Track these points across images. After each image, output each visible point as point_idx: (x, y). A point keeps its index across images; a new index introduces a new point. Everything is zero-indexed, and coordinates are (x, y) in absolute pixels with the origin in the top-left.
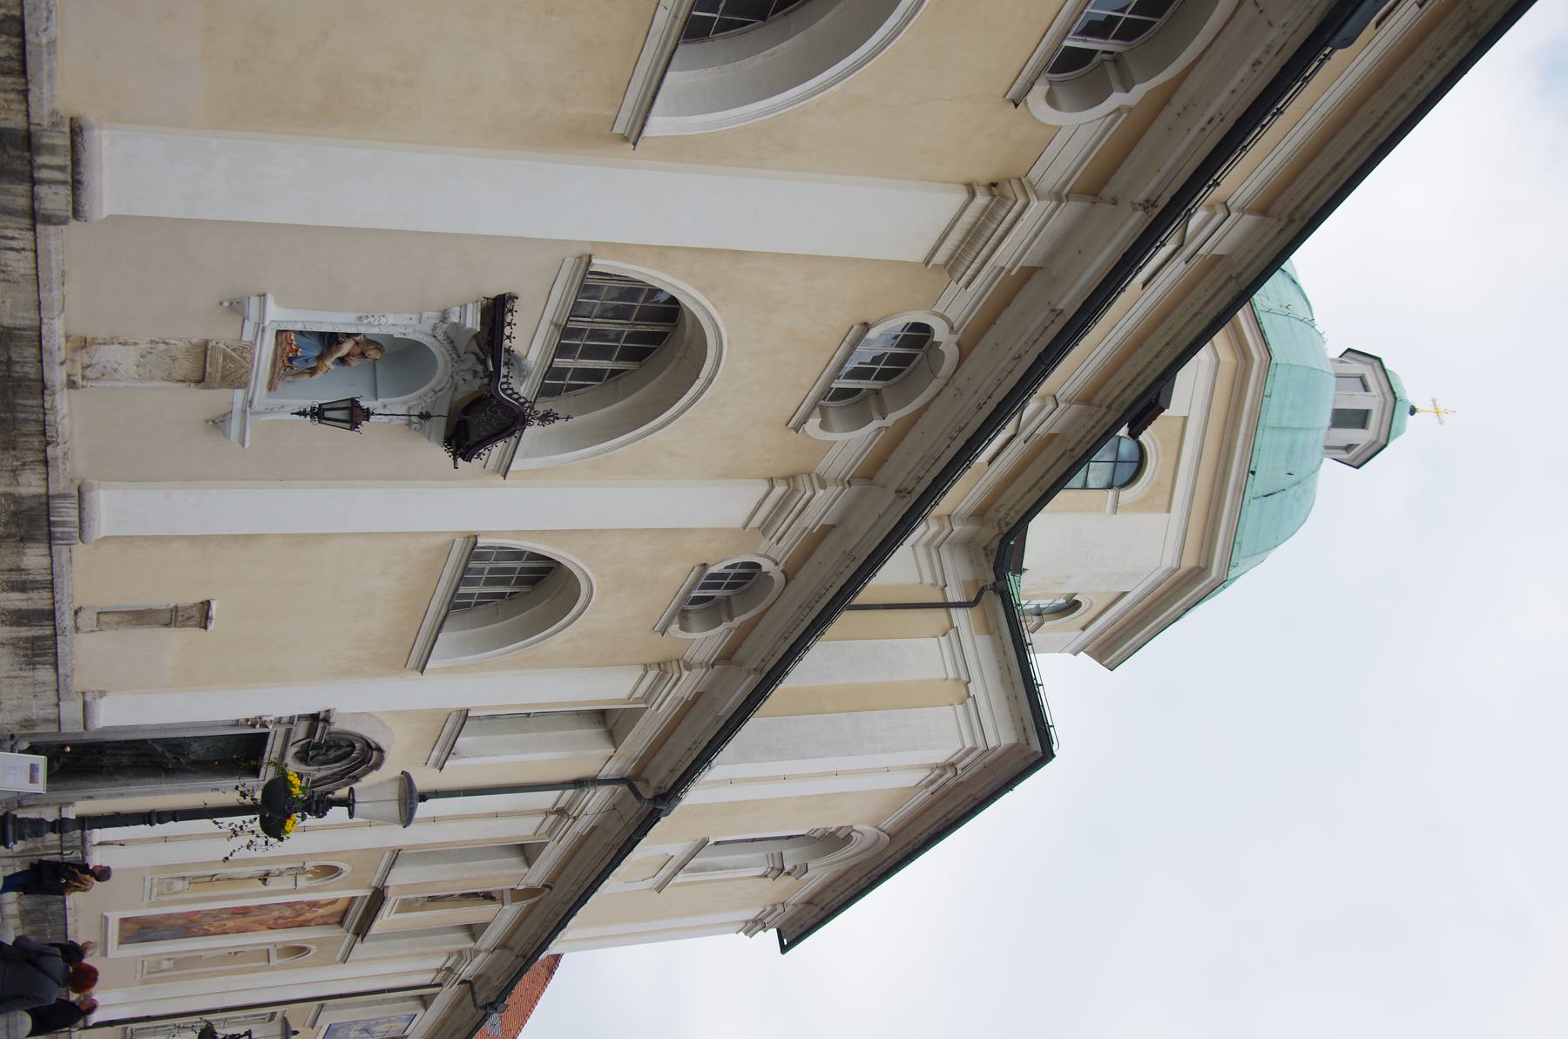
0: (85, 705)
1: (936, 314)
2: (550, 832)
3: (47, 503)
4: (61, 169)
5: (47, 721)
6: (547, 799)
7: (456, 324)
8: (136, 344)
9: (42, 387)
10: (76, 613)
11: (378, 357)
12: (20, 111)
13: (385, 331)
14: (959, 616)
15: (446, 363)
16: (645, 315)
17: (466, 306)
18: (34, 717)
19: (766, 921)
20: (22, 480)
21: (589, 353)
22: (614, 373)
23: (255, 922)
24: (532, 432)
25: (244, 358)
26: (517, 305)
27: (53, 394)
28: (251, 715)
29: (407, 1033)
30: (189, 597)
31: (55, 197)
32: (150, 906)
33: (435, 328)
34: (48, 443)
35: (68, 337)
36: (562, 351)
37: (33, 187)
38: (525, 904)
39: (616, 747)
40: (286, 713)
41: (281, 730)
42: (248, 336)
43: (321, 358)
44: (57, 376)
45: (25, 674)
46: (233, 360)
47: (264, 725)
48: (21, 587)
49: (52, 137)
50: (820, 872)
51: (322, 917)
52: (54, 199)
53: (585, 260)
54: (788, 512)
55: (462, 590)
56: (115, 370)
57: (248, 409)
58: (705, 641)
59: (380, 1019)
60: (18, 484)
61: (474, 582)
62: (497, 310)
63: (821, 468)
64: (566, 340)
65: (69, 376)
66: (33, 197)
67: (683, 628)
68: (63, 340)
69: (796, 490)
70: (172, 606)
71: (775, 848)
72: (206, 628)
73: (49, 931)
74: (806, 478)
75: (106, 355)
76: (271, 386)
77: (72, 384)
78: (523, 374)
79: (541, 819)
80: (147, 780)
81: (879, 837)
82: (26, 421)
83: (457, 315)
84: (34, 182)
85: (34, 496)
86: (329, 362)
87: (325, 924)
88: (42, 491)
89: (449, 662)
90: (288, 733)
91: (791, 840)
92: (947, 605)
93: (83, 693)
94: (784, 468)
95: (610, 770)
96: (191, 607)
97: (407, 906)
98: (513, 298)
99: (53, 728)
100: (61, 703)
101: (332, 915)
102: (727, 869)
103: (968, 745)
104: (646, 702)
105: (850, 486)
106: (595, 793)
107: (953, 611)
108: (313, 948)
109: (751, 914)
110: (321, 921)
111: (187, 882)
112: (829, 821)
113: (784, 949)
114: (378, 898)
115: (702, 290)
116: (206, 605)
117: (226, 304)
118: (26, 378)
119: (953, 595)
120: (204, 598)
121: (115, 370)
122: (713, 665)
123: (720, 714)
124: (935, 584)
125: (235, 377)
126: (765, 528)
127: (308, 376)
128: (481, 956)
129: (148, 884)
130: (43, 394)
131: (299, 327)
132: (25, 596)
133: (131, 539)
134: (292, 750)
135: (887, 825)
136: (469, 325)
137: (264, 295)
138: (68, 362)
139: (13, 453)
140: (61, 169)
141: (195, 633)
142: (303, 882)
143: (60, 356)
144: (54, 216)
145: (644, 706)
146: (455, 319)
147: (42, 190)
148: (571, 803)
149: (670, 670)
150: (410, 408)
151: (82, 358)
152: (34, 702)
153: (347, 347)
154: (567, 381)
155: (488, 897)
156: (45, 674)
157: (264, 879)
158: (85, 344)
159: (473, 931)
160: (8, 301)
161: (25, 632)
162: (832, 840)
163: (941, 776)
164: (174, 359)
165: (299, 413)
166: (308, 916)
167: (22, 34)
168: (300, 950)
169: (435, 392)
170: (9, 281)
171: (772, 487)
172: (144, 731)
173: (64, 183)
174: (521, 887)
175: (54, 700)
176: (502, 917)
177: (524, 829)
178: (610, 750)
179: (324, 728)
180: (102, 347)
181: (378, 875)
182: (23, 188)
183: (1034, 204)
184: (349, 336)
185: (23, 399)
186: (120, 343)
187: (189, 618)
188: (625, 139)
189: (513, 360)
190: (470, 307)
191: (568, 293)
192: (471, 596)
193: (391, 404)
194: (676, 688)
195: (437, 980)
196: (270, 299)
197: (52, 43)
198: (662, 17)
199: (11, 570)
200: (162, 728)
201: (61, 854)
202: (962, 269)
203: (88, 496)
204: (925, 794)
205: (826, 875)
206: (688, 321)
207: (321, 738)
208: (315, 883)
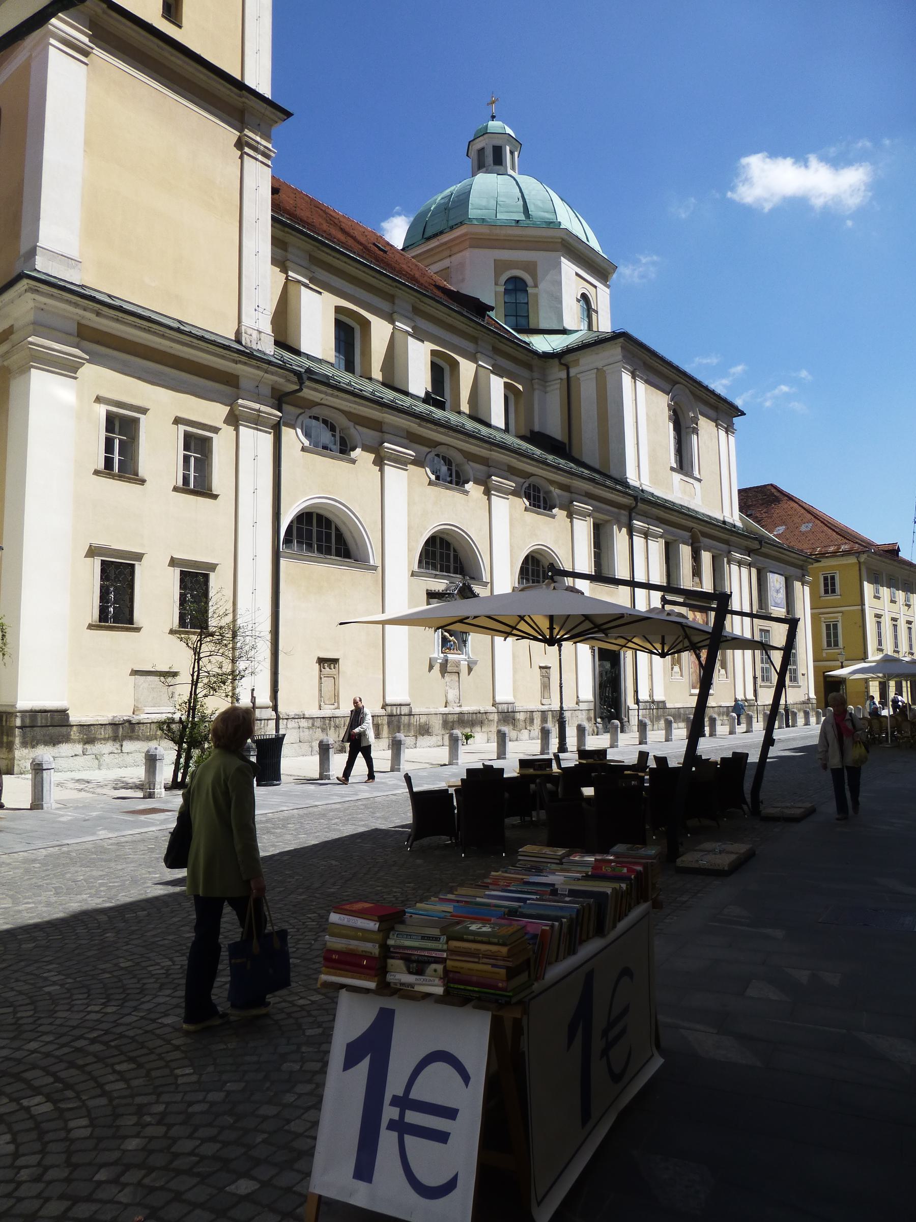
4: (397, 708)
5: (588, 713)
14: (573, 372)
44: (458, 710)
48: (532, 721)
52: (405, 710)
98: (427, 590)
99: (592, 712)
119: (563, 375)
140: (397, 708)
164: (452, 680)
201: (653, 709)
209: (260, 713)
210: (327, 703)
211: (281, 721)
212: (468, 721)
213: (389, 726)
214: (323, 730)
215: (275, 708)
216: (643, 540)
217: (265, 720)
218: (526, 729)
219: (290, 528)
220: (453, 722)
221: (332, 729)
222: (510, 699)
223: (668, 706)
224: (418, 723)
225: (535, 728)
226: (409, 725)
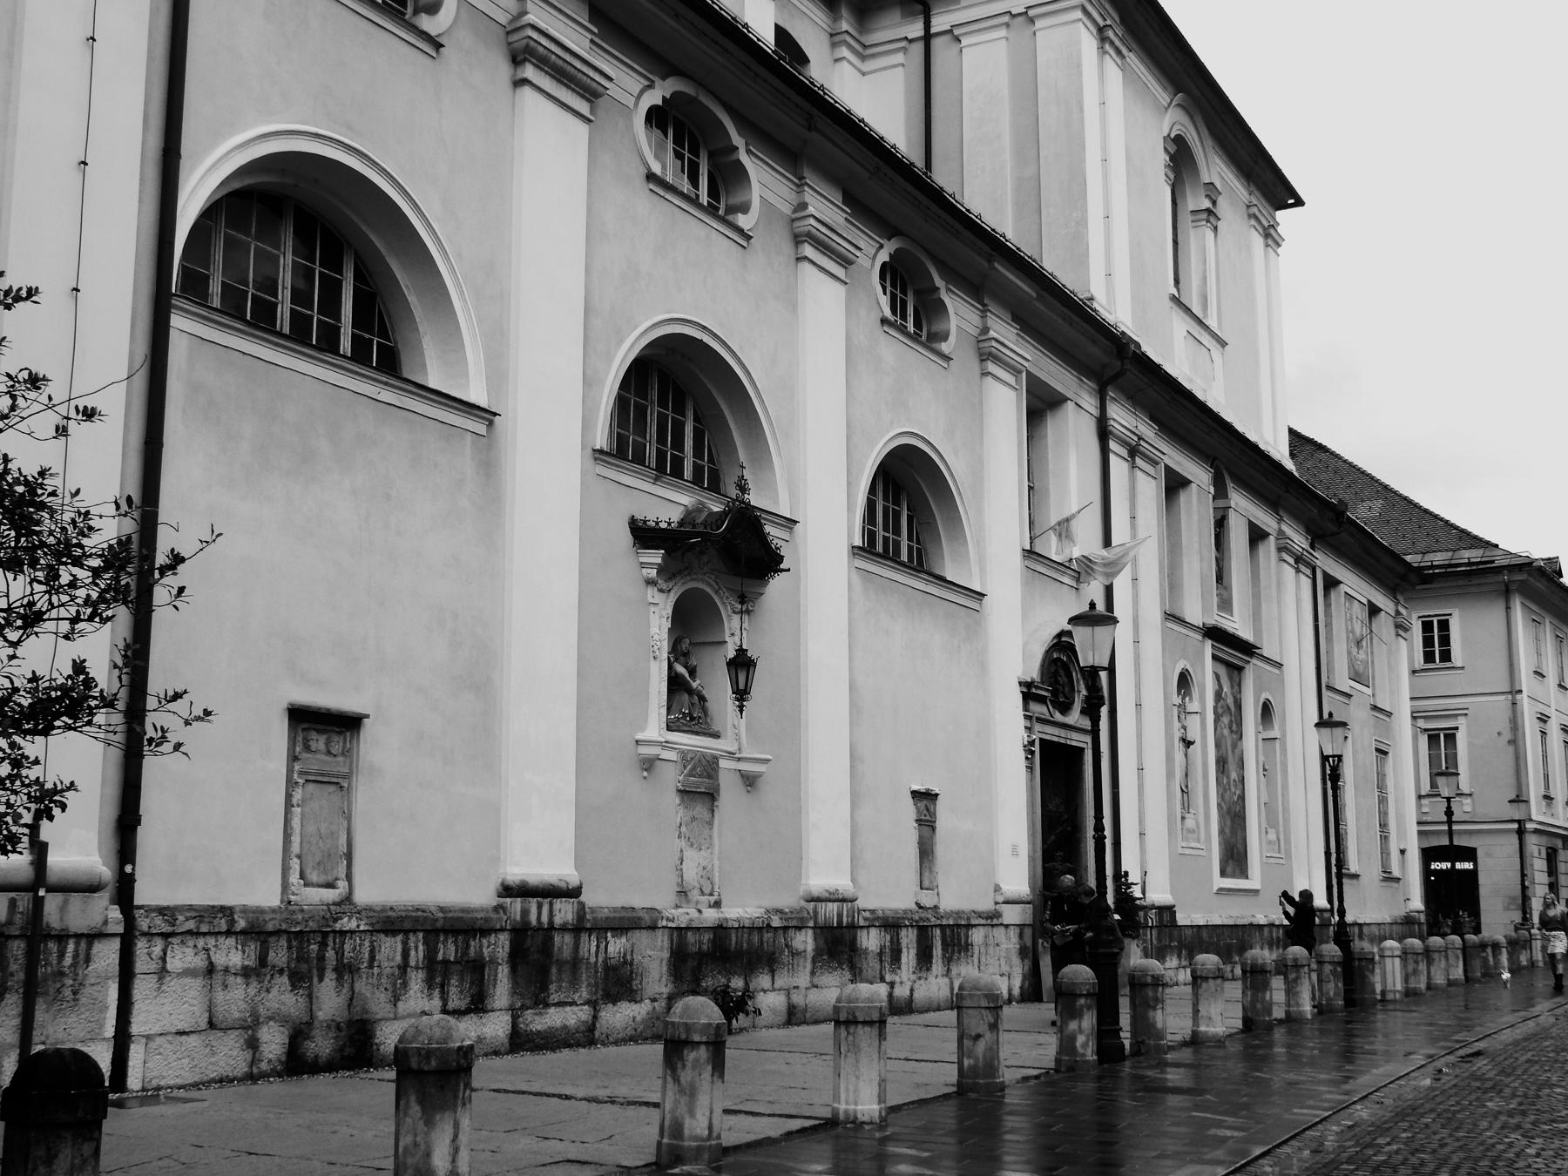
0: (1007, 902)
1: (636, 104)
2: (1154, 463)
3: (821, 928)
4: (540, 907)
5: (1021, 936)
6: (1118, 467)
7: (658, 573)
8: (681, 851)
9: (720, 930)
10: (921, 907)
11: (688, 641)
12: (496, 937)
13: (666, 636)
15: (693, 580)
16: (643, 392)
17: (642, 563)
18: (1018, 946)
19: (1266, 225)
20: (801, 947)
21: (678, 444)
22: (696, 419)
23: (1233, 751)
24: (755, 499)
25: (692, 758)
26: (640, 516)
27: (726, 920)
28: (1022, 755)
29: (1365, 602)
30: (908, 810)
31: (563, 912)
32: (1210, 850)
33: (661, 591)
34: (769, 925)
35: (677, 907)
36: (677, 472)
37: (556, 929)
38: (1230, 485)
39: (1064, 399)
40: (1022, 722)
41: (1038, 727)
42: (672, 755)
43: (690, 691)
44: (711, 916)
45: (976, 952)
46: (694, 768)
47: (1032, 743)
49: (515, 913)
50: (1214, 168)
51: (1232, 687)
52: (564, 911)
53: (597, 456)
54: (830, 242)
55: (904, 557)
56: (704, 868)
57: (737, 756)
58: (960, 314)
59: (1347, 629)
60: (805, 951)
61: (897, 545)
62: (643, 534)
63: (786, 209)
64: (666, 469)
65: (710, 907)
66: (564, 929)
67: (945, 337)
68: (680, 910)
69: (809, 235)
70: (916, 825)
71: (1185, 219)
72: (937, 795)
74: (797, 224)
75: (691, 874)
76: (716, 736)
77: (717, 904)
78: (700, 508)
79: (1139, 474)
80: (1082, 850)
81: (1178, 105)
82: (750, 942)
83: (649, 571)
84: (551, 927)
85: (815, 939)
86: (695, 685)
87: (1240, 685)
88: (810, 932)
89: (975, 569)
90: (1041, 720)
91: (1178, 201)
92: (928, 38)
93: (996, 903)
94: (787, 246)
95: (1090, 403)
96: (917, 808)
97: (1225, 605)
99: (1028, 932)
100: (1005, 923)
101: (1231, 678)
102: (1205, 271)
103: (1079, 14)
104: (1020, 372)
105: (804, 178)
106: (1114, 420)
107: (933, 30)
108: (1264, 696)
109: (1258, 240)
110: (1236, 688)
111: (1187, 815)
112: (1157, 161)
113: (1299, 202)
114: (1215, 634)
115: (621, 341)
116: (916, 795)
117: (645, 774)
118: (713, 942)
121: (704, 868)
122: (984, 305)
123: (1034, 295)
124: (904, 49)
125: (707, 767)
126: (845, 262)
127: (706, 703)
128: (1285, 528)
129: (1188, 851)
130: (726, 928)
131: (664, 710)
132: (904, 950)
133: (854, 859)
134: (1058, 717)
135: (1163, 97)
136: (659, 560)
137: (637, 741)
138: (699, 907)
139: (777, 955)
140: (540, 907)
141: (942, 807)
143: (694, 913)
144: (578, 913)
145: (1024, 374)
146: (653, 573)
147: (558, 920)
148: (1123, 442)
149: (987, 350)
150: (734, 612)
151: (695, 895)
152: (1004, 946)
153: (680, 669)
154: (705, 463)
155: (1221, 524)
156: (977, 936)
157: (1188, 744)
158: (683, 893)
159: (1257, 535)
160: (649, 952)
161: (937, 951)
162: (1180, 159)
163: (1112, 43)
164: (694, 819)
165: (741, 711)
166: (1230, 701)
167: (436, 931)
168: (1266, 710)
169: (720, 588)
170: (632, 951)
171: (806, 258)
172: (1034, 851)
173: (551, 905)
174: (1212, 490)
175: (1002, 929)
176: (1242, 507)
177: (1150, 489)
178: (1070, 405)
179: (1037, 687)
180: (685, 878)
181: (1191, 634)
182: (557, 939)
183: (531, 18)
184: (670, 667)
185: (731, 944)
186: (681, 863)
187: (928, 810)
188: (491, 423)
189: (688, 517)
190: (643, 560)
191: (628, 469)
192: (910, 549)
193: (730, 629)
194: (1006, 342)
195: (1308, 572)
196: (639, 736)
197: (441, 909)
198: (387, 396)
199: (881, 961)
200: (1032, 835)
201: (1151, 928)
202: (594, 85)
203: (816, 892)
204: (1133, 59)
205: (1218, 160)
206: (647, 352)
207: (1047, 690)
208: (1195, 693)
209: (63, 908)
210: (314, 877)
211: (141, 945)
212: (739, 954)
213: (514, 970)
214: (299, 978)
215: (124, 890)
216: (1125, 466)
217: (78, 936)
218: (882, 979)
219: (210, 214)
220: (701, 956)
221: (330, 976)
222: (840, 882)
223: (1182, 919)
224: (600, 960)
225: (905, 979)
226: (576, 962)
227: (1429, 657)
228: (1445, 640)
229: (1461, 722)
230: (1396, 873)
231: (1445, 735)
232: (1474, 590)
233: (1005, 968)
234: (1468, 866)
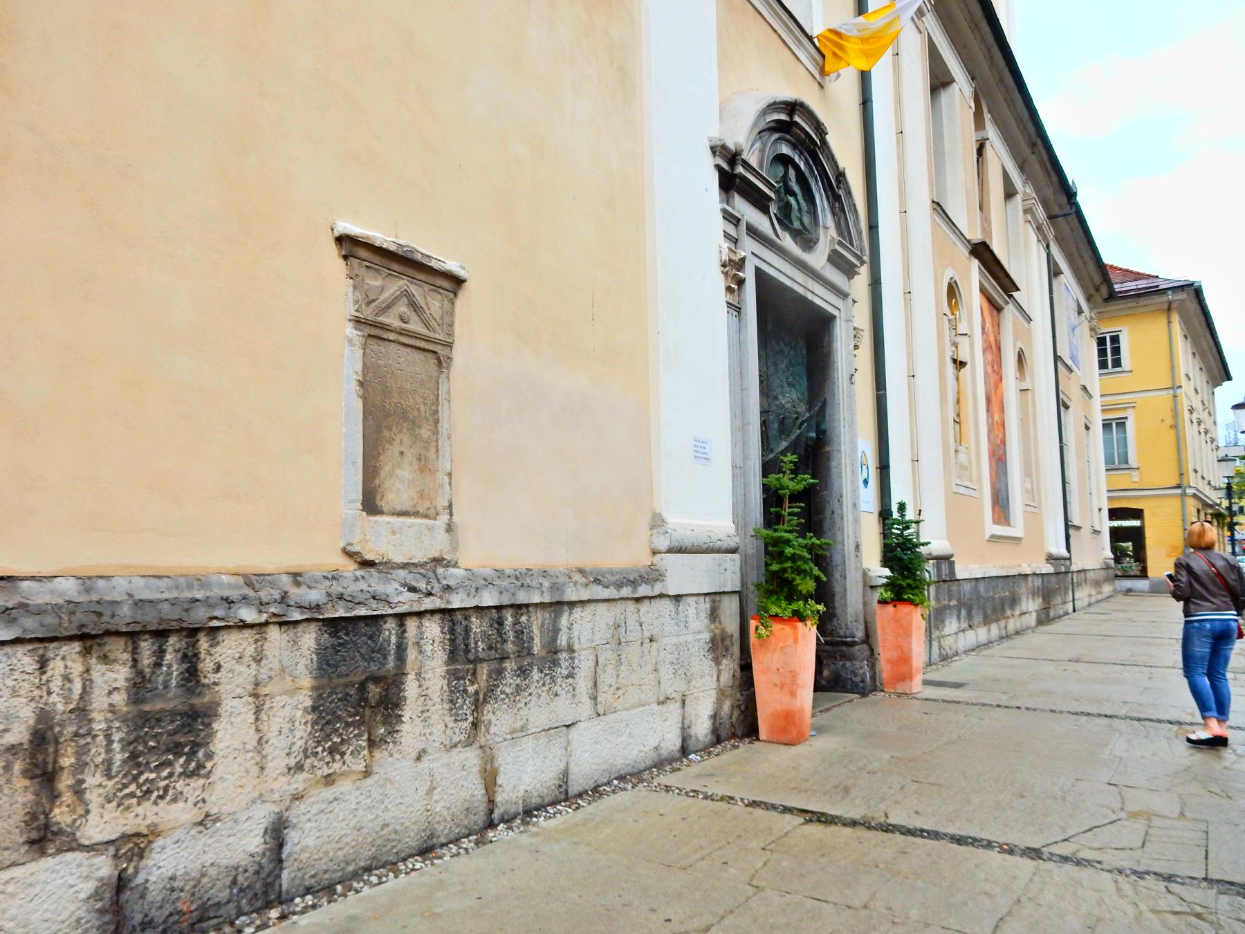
5: (714, 615)
18: (707, 636)
23: (995, 392)
40: (719, 224)
73: (1002, 594)
80: (834, 470)
87: (999, 325)
93: (655, 552)
99: (730, 607)
101: (992, 316)
108: (1019, 345)
110: (996, 328)
111: (960, 448)
120: (332, 251)
129: (962, 490)
142: (962, 328)
152: (668, 642)
155: (980, 151)
157: (959, 364)
166: (992, 338)
168: (1021, 358)
175: (666, 606)
179: (746, 165)
181: (959, 244)
227: (1103, 365)
228: (1116, 351)
229: (1130, 413)
230: (1097, 528)
231: (1117, 424)
232: (1140, 310)
233: (672, 686)
234: (1136, 523)
